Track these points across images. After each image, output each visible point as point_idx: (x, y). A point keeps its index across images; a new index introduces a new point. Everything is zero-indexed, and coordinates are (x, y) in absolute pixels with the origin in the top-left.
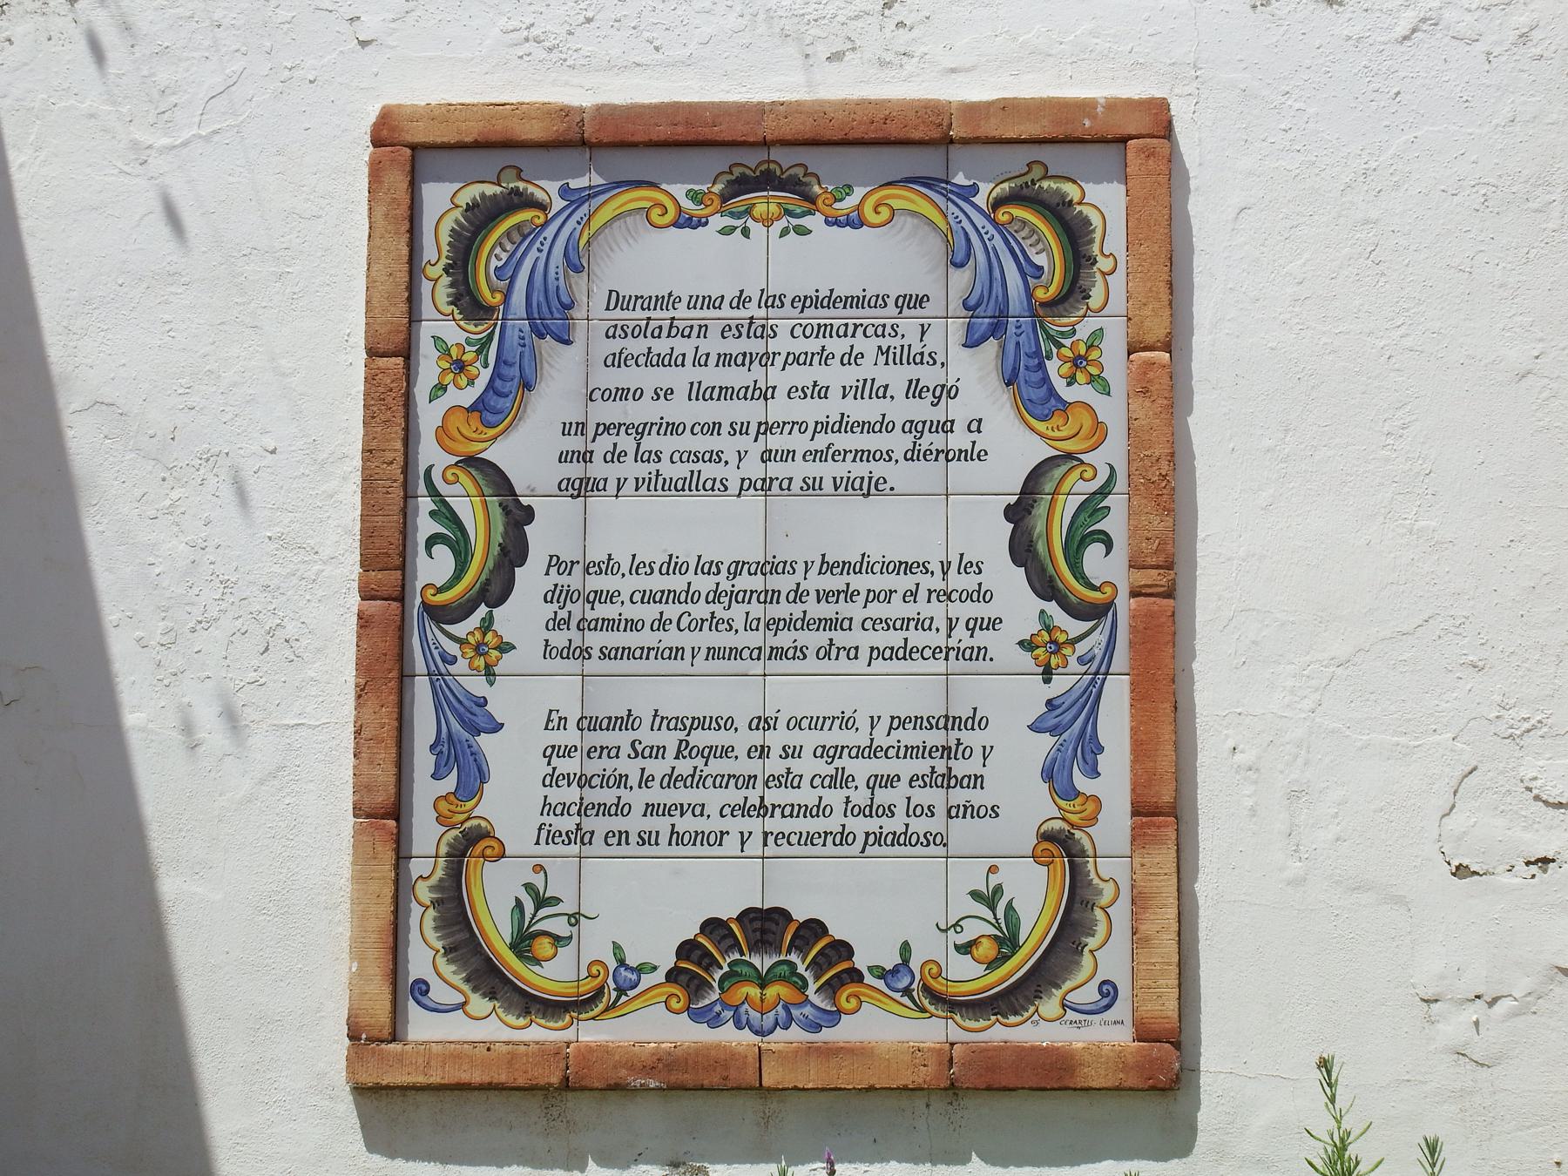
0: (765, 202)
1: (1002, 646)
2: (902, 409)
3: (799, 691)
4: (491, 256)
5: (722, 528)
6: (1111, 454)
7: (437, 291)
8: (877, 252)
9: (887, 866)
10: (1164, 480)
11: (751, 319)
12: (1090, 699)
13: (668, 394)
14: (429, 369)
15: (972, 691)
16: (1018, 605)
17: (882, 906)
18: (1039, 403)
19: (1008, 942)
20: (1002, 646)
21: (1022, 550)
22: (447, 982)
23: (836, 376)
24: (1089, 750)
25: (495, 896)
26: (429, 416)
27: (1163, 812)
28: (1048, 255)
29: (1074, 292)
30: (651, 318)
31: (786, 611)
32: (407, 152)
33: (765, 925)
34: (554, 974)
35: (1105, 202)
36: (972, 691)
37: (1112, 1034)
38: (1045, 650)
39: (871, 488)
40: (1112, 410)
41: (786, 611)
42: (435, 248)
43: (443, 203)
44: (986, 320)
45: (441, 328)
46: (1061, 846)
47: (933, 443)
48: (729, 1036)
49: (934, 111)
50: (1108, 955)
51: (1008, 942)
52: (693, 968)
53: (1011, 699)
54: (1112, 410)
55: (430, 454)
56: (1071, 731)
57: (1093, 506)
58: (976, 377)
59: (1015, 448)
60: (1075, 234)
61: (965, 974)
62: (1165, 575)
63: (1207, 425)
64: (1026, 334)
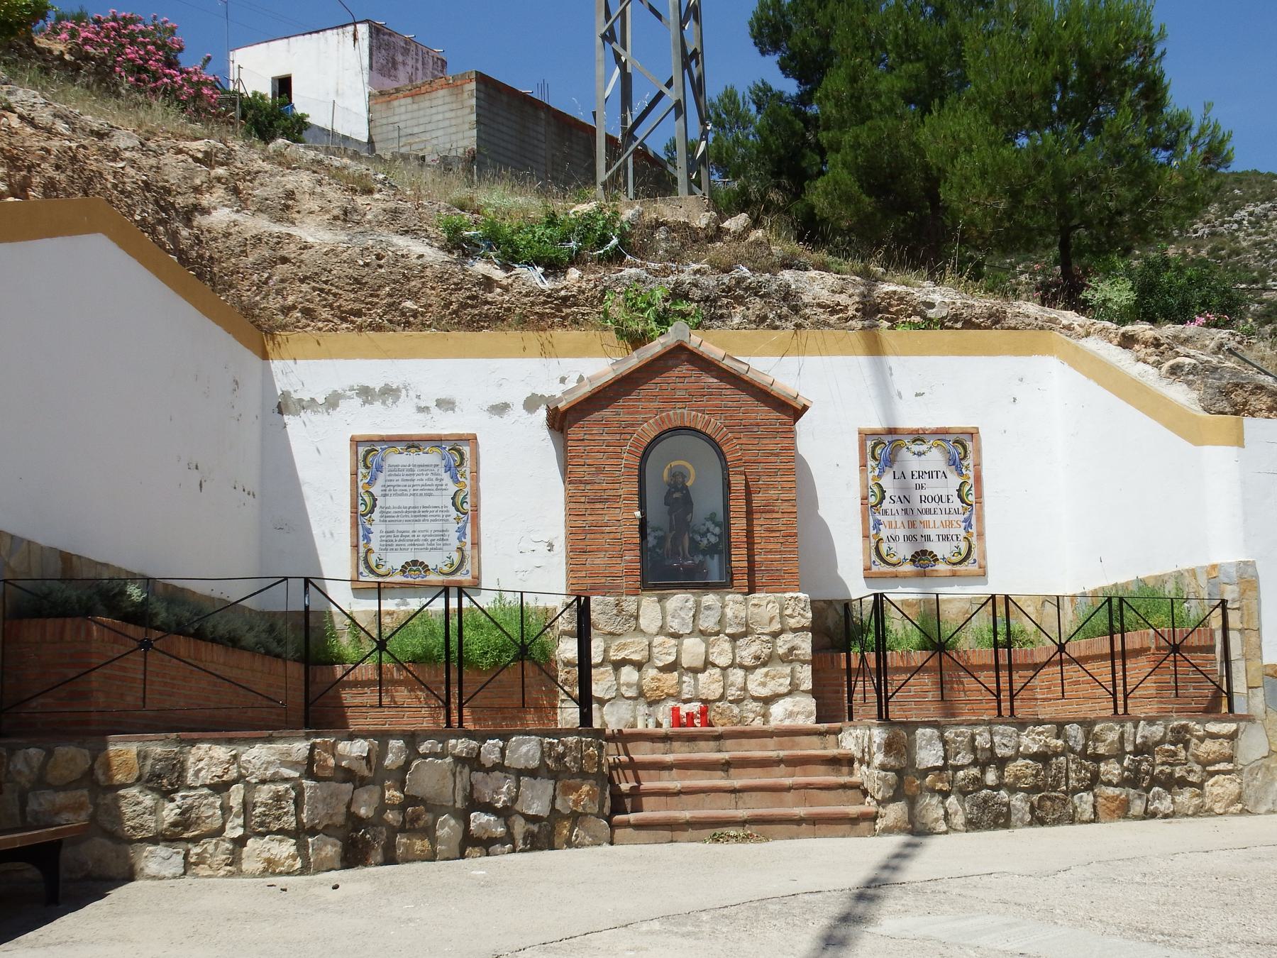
0: (413, 450)
1: (451, 519)
2: (435, 482)
3: (419, 526)
4: (370, 458)
5: (407, 501)
6: (467, 489)
7: (361, 464)
8: (430, 458)
9: (434, 553)
10: (476, 493)
11: (411, 469)
12: (464, 527)
13: (398, 480)
14: (360, 476)
15: (446, 526)
16: (454, 513)
17: (434, 559)
18: (456, 481)
19: (452, 564)
20: (451, 519)
21: (454, 504)
22: (366, 572)
23: (424, 477)
24: (464, 534)
25: (373, 559)
26: (360, 484)
27: (476, 544)
28: (457, 458)
29: (461, 464)
30: (395, 469)
31: (417, 514)
32: (356, 442)
33: (415, 563)
34: (382, 571)
35: (466, 450)
36: (446, 526)
37: (469, 578)
38: (458, 520)
39: (430, 495)
40: (468, 482)
41: (417, 514)
42: (361, 458)
43: (362, 450)
44: (448, 468)
45: (362, 470)
46: (460, 549)
47: (440, 488)
48: (410, 579)
49: (439, 435)
50: (468, 566)
51: (452, 564)
52: (404, 570)
53: (452, 527)
54: (468, 482)
55: (361, 490)
56: (462, 532)
57: (465, 497)
58: (446, 477)
59: (453, 488)
60: (461, 455)
61: (446, 569)
62: (476, 508)
63: (483, 484)
64: (454, 470)
